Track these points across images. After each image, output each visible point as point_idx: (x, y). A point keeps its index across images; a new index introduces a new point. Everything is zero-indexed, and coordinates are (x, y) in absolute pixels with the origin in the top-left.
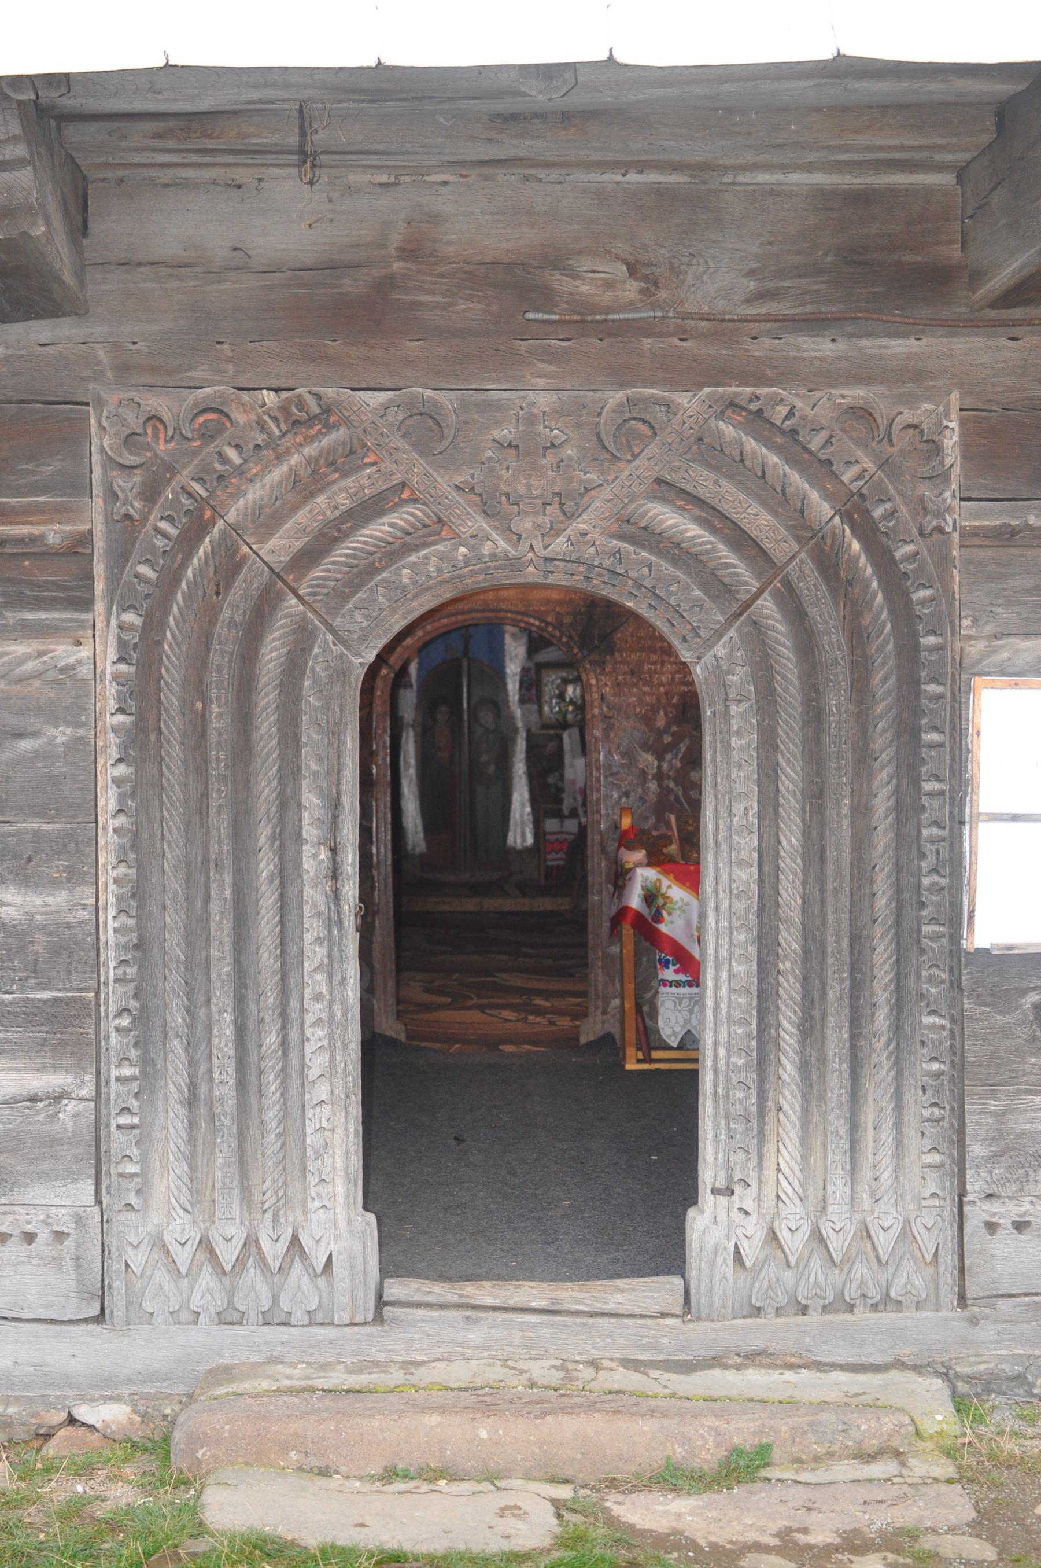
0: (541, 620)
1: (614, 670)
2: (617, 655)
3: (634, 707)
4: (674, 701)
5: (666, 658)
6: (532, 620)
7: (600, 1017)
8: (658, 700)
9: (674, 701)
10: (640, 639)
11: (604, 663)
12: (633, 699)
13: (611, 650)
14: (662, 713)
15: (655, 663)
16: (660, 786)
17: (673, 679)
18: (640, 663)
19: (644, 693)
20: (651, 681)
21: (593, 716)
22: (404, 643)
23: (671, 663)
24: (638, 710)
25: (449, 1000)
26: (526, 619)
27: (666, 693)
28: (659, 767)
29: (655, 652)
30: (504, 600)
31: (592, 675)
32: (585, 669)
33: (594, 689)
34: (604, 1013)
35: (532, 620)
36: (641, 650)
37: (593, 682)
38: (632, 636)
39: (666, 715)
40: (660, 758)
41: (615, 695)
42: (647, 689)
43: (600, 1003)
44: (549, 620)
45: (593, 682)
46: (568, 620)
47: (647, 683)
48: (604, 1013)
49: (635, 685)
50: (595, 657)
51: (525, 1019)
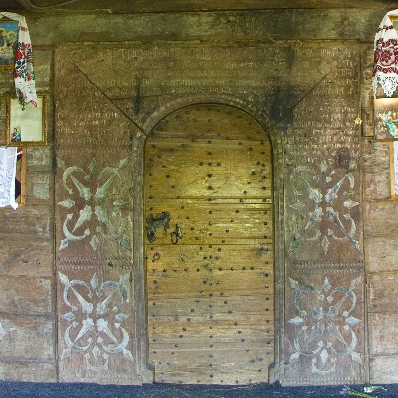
0: (244, 100)
1: (293, 132)
2: (295, 123)
4: (333, 154)
5: (327, 126)
6: (238, 100)
7: (283, 366)
8: (323, 153)
9: (333, 154)
10: (310, 112)
11: (287, 129)
15: (320, 129)
16: (324, 211)
17: (332, 139)
19: (313, 149)
20: (318, 141)
21: (279, 164)
22: (153, 116)
23: (331, 129)
24: (309, 160)
26: (234, 99)
28: (323, 198)
29: (320, 121)
30: (219, 87)
33: (280, 146)
34: (286, 363)
35: (238, 100)
37: (279, 141)
39: (328, 163)
40: (324, 193)
41: (294, 150)
42: (315, 146)
43: (283, 357)
44: (249, 99)
46: (261, 99)
48: (286, 363)
49: (306, 143)
50: (281, 125)
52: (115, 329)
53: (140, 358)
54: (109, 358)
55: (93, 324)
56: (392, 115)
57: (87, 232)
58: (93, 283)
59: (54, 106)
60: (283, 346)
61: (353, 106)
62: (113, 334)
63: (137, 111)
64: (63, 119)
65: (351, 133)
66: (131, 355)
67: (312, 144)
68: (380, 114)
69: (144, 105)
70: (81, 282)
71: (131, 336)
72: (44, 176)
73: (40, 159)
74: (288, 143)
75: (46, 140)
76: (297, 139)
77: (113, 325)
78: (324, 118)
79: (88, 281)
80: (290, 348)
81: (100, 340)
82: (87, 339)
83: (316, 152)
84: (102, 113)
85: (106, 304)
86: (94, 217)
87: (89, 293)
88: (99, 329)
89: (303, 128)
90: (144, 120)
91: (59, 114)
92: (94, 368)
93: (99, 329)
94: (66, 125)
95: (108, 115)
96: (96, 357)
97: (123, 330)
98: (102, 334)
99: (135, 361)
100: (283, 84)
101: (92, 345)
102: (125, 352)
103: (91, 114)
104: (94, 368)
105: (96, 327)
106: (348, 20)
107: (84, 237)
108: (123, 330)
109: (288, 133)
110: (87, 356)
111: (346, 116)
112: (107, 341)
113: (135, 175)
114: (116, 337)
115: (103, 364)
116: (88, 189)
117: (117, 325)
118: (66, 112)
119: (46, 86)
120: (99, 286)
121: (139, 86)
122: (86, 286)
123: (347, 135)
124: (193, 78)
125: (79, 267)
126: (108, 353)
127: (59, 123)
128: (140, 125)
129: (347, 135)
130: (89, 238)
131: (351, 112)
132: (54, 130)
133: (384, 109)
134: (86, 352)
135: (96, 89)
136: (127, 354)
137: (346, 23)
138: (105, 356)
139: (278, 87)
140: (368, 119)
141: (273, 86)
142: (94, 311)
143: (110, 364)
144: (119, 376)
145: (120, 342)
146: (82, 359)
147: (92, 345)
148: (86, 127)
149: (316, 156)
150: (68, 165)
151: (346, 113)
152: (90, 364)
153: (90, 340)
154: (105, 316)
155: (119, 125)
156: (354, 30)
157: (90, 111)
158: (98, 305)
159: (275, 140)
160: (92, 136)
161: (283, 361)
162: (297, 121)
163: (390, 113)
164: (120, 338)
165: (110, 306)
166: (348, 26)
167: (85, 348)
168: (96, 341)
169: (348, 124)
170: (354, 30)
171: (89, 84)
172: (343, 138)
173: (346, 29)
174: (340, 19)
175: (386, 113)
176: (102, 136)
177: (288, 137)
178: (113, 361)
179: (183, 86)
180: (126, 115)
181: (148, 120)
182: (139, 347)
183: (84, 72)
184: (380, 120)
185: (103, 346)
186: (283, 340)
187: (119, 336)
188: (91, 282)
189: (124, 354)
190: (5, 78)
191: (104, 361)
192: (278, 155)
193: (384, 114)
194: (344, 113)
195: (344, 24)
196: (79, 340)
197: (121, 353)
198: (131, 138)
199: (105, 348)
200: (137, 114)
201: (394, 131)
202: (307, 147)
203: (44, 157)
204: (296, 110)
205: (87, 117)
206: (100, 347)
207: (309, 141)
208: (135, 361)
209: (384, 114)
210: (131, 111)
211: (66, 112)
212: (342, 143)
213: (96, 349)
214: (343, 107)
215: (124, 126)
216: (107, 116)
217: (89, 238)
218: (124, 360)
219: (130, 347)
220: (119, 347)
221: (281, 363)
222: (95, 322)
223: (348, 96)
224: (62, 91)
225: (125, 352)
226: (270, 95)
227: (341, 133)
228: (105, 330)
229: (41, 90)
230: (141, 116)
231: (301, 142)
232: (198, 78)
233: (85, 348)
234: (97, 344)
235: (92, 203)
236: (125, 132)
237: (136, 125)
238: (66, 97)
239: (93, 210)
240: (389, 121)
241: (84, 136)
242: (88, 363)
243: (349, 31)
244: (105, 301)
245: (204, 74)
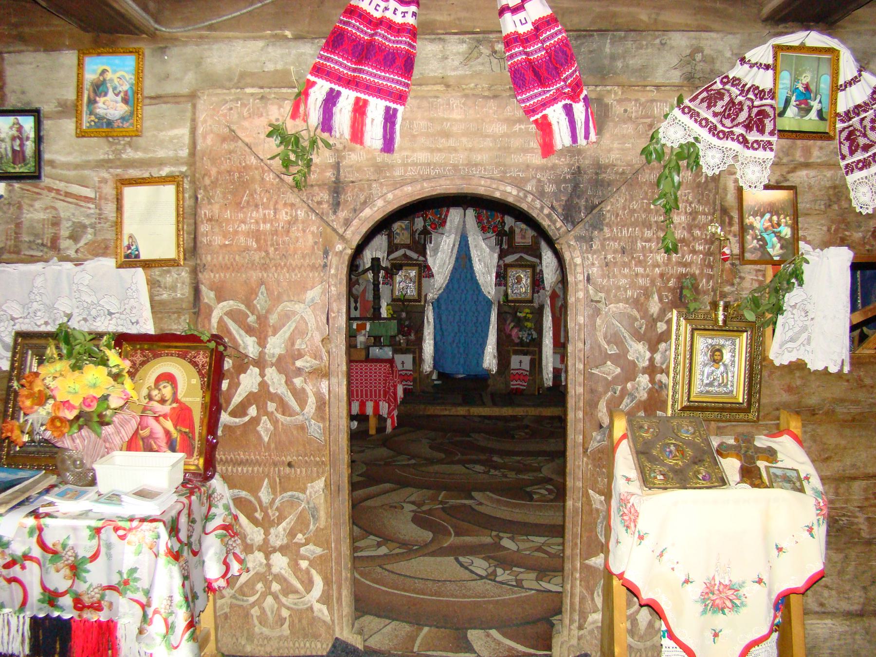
0: (520, 189)
1: (603, 246)
2: (606, 229)
3: (626, 290)
4: (671, 284)
6: (509, 189)
7: (575, 632)
8: (653, 282)
9: (671, 284)
10: (633, 211)
11: (591, 239)
12: (623, 282)
13: (598, 225)
14: (656, 297)
15: (649, 240)
16: (652, 381)
18: (633, 240)
19: (637, 275)
20: (645, 261)
21: (577, 300)
22: (362, 215)
24: (629, 293)
25: (428, 535)
26: (502, 188)
27: (662, 275)
28: (652, 360)
29: (649, 227)
30: (476, 165)
31: (577, 253)
32: (569, 246)
33: (579, 269)
35: (509, 189)
36: (634, 225)
37: (578, 261)
38: (624, 208)
39: (661, 300)
40: (653, 349)
42: (640, 270)
43: (576, 617)
45: (578, 261)
46: (550, 188)
47: (639, 263)
48: (580, 628)
49: (625, 265)
50: (579, 230)
51: (494, 573)
52: (300, 569)
53: (341, 617)
54: (290, 616)
55: (265, 562)
56: (770, 220)
57: (253, 411)
58: (265, 495)
59: (197, 198)
60: (577, 600)
61: (707, 203)
62: (297, 577)
63: (336, 205)
64: (210, 220)
65: (701, 248)
66: (326, 612)
67: (636, 265)
68: (751, 217)
69: (348, 196)
70: (243, 494)
71: (327, 582)
72: (179, 317)
73: (173, 288)
74: (593, 264)
75: (182, 256)
76: (609, 257)
77: (297, 564)
78: (656, 222)
79: (254, 491)
80: (589, 604)
81: (275, 587)
82: (254, 585)
83: (641, 281)
84: (276, 211)
85: (284, 530)
86: (263, 385)
87: (256, 511)
88: (275, 570)
89: (620, 239)
90: (347, 223)
91: (204, 211)
92: (266, 631)
93: (275, 570)
94: (216, 230)
95: (287, 213)
96: (269, 613)
97: (313, 572)
98: (279, 578)
99: (333, 621)
100: (587, 162)
101: (264, 596)
102: (317, 606)
103: (257, 211)
104: (266, 631)
105: (269, 566)
106: (702, 53)
107: (247, 419)
108: (313, 572)
109: (594, 247)
110: (255, 612)
111: (694, 219)
112: (288, 590)
113: (333, 315)
114: (302, 583)
115: (282, 625)
116: (254, 339)
117: (304, 564)
118: (216, 209)
119: (182, 164)
120: (273, 500)
121: (338, 163)
122: (252, 499)
123: (694, 252)
124: (432, 150)
125: (240, 469)
126: (288, 608)
127: (204, 228)
128: (341, 231)
129: (694, 252)
130: (255, 421)
131: (704, 213)
132: (195, 238)
133: (759, 210)
134: (253, 605)
135: (266, 168)
136: (320, 611)
137: (699, 57)
138: (285, 613)
139: (579, 167)
140: (731, 224)
141: (570, 166)
142: (266, 541)
143: (292, 626)
144: (308, 645)
145: (308, 591)
146: (247, 615)
147: (264, 596)
148: (248, 234)
149: (641, 288)
150: (220, 299)
151: (694, 214)
152: (260, 623)
153: (260, 586)
154: (283, 550)
155: (304, 231)
156: (712, 71)
157: (257, 206)
158: (272, 531)
159: (572, 258)
160: (259, 249)
161: (576, 624)
162: (609, 225)
163: (767, 216)
164: (309, 585)
165: (292, 534)
166: (701, 64)
167: (252, 599)
168: (270, 588)
169: (697, 233)
170: (712, 71)
171: (253, 161)
172: (688, 258)
173: (698, 68)
174: (688, 52)
175: (762, 216)
176: (276, 250)
177: (595, 252)
178: (296, 621)
179: (414, 164)
180: (317, 214)
181: (355, 222)
182: (339, 599)
183: (247, 140)
184: (752, 227)
185: (281, 596)
186: (578, 590)
187: (306, 581)
188: (260, 494)
189: (315, 609)
190: (113, 152)
191: (282, 621)
192: (576, 284)
193: (758, 218)
194: (690, 214)
195: (694, 60)
196: (241, 587)
197: (311, 608)
198: (326, 253)
199: (284, 600)
200: (335, 213)
201: (773, 247)
202: (626, 271)
203: (179, 285)
204: (609, 208)
205: (251, 218)
206: (276, 598)
207: (630, 261)
208: (333, 621)
209: (758, 218)
210: (325, 206)
211: (216, 209)
212: (685, 265)
213: (270, 600)
214: (690, 203)
215: (313, 233)
216: (284, 216)
217: (255, 421)
218: (314, 620)
219: (325, 599)
220: (306, 599)
221: (572, 627)
222: (267, 558)
223: (699, 185)
224: (207, 174)
225: (317, 606)
226: (565, 181)
227: (685, 248)
228: (283, 572)
229: (173, 172)
230: (343, 214)
231: (615, 263)
232: (439, 150)
233: (252, 599)
234: (271, 593)
235: (260, 363)
236: (316, 243)
237: (334, 230)
238: (214, 184)
239: (262, 375)
240: (766, 229)
241: (247, 249)
242: (256, 622)
243: (703, 72)
244: (284, 524)
245: (452, 142)
